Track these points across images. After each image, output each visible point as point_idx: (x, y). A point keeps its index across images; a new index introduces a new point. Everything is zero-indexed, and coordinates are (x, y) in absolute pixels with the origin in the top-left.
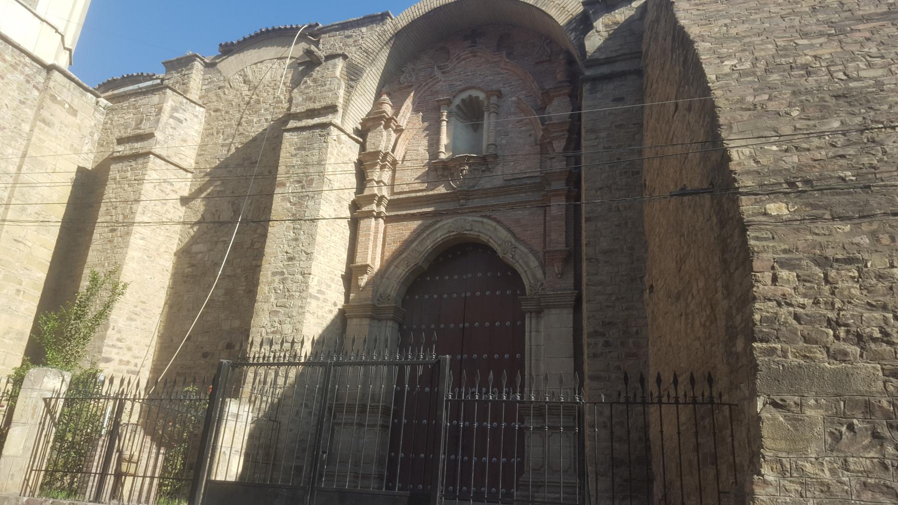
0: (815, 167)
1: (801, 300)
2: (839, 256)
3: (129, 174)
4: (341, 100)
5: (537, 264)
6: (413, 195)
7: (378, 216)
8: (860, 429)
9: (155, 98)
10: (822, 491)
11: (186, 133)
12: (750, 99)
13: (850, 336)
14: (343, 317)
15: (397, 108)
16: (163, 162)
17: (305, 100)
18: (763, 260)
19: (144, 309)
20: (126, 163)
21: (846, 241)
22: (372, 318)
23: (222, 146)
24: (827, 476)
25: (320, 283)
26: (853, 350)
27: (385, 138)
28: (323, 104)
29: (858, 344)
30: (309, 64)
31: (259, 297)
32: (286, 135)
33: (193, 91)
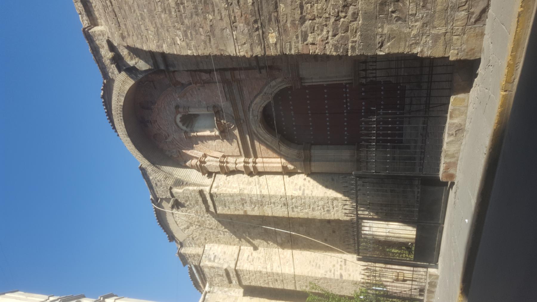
0: (246, 17)
1: (325, 33)
2: (299, 12)
3: (247, 277)
4: (195, 188)
5: (274, 82)
6: (241, 146)
7: (255, 163)
8: (394, 8)
9: (206, 270)
10: (426, 26)
11: (221, 253)
12: (203, 37)
13: (344, 10)
14: (311, 174)
15: (192, 158)
16: (238, 262)
17: (198, 205)
18: (303, 49)
19: (314, 261)
20: (242, 278)
21: (290, 8)
22: (310, 161)
23: (224, 235)
24: (418, 24)
25: (296, 190)
26: (351, 9)
27: (211, 163)
28: (198, 196)
29: (348, 7)
30: (177, 205)
31: (306, 217)
32: (218, 212)
33: (197, 251)
